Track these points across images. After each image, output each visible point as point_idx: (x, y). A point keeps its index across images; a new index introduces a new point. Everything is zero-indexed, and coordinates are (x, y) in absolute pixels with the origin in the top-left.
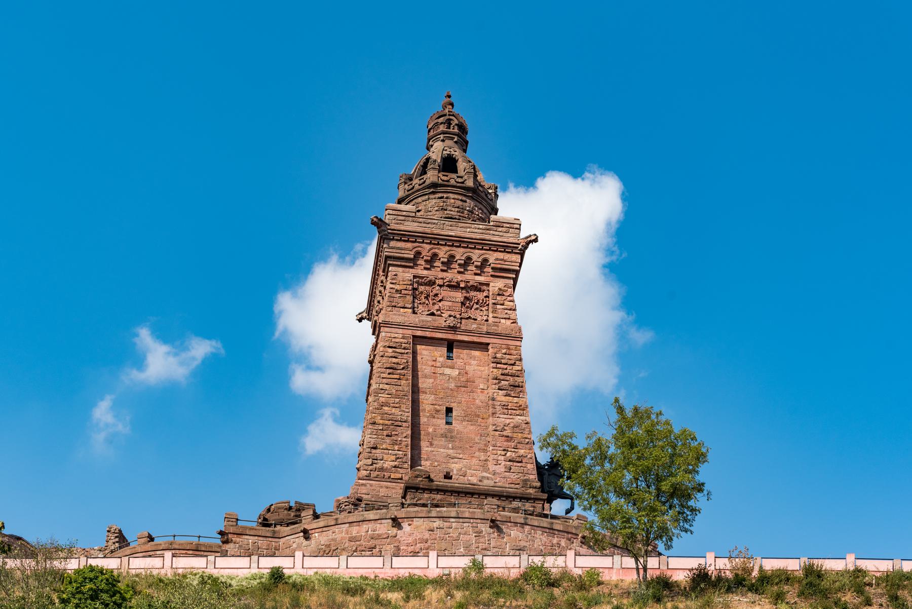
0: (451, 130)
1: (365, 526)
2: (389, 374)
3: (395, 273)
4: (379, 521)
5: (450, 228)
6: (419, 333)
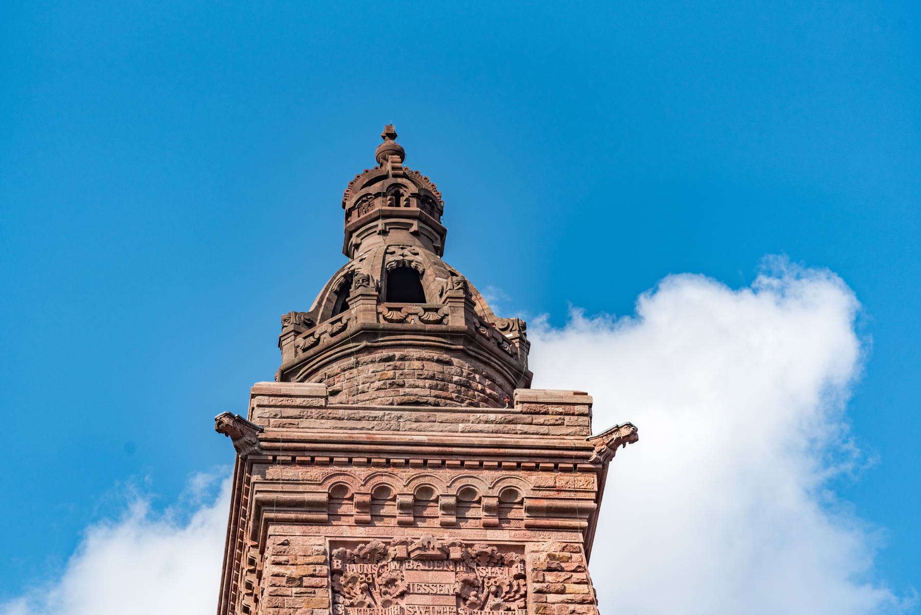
0: (402, 208)
3: (283, 539)
5: (415, 425)
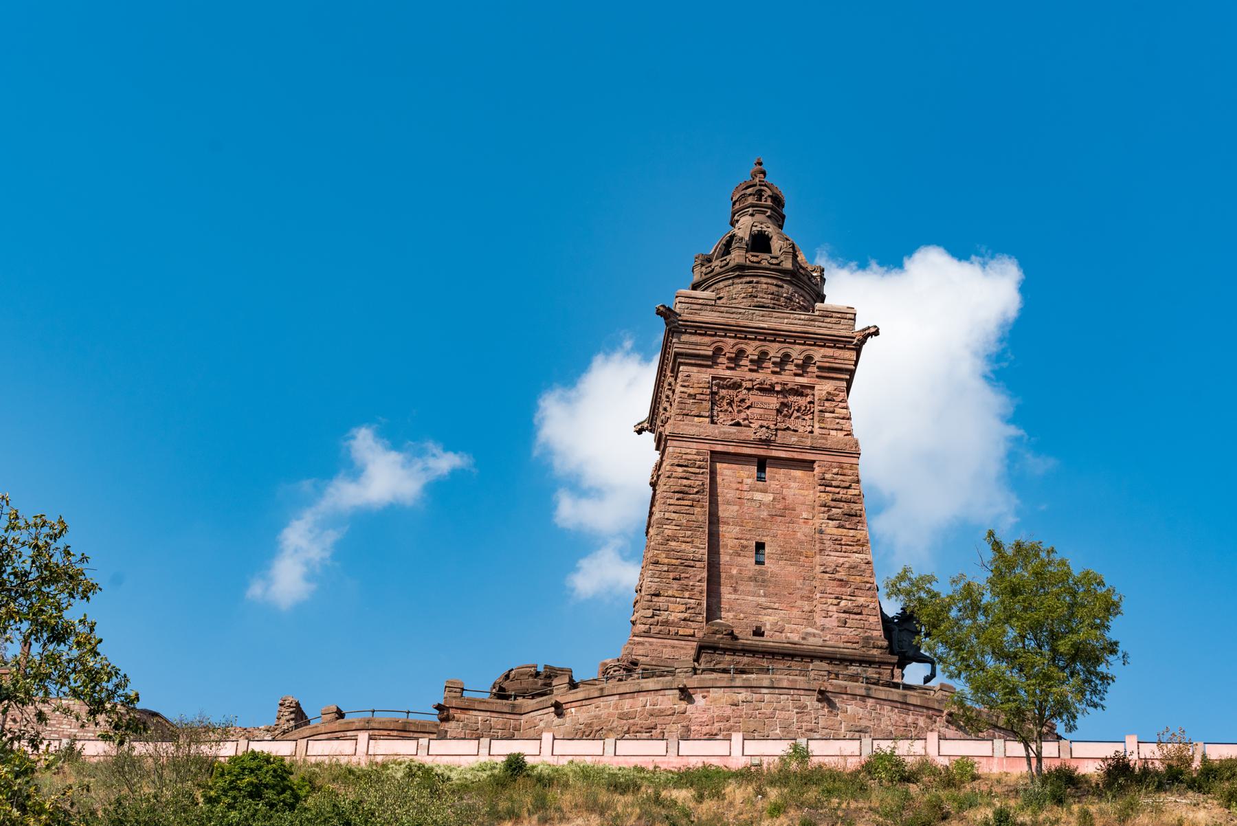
0: (763, 203)
1: (641, 699)
2: (678, 499)
4: (662, 692)
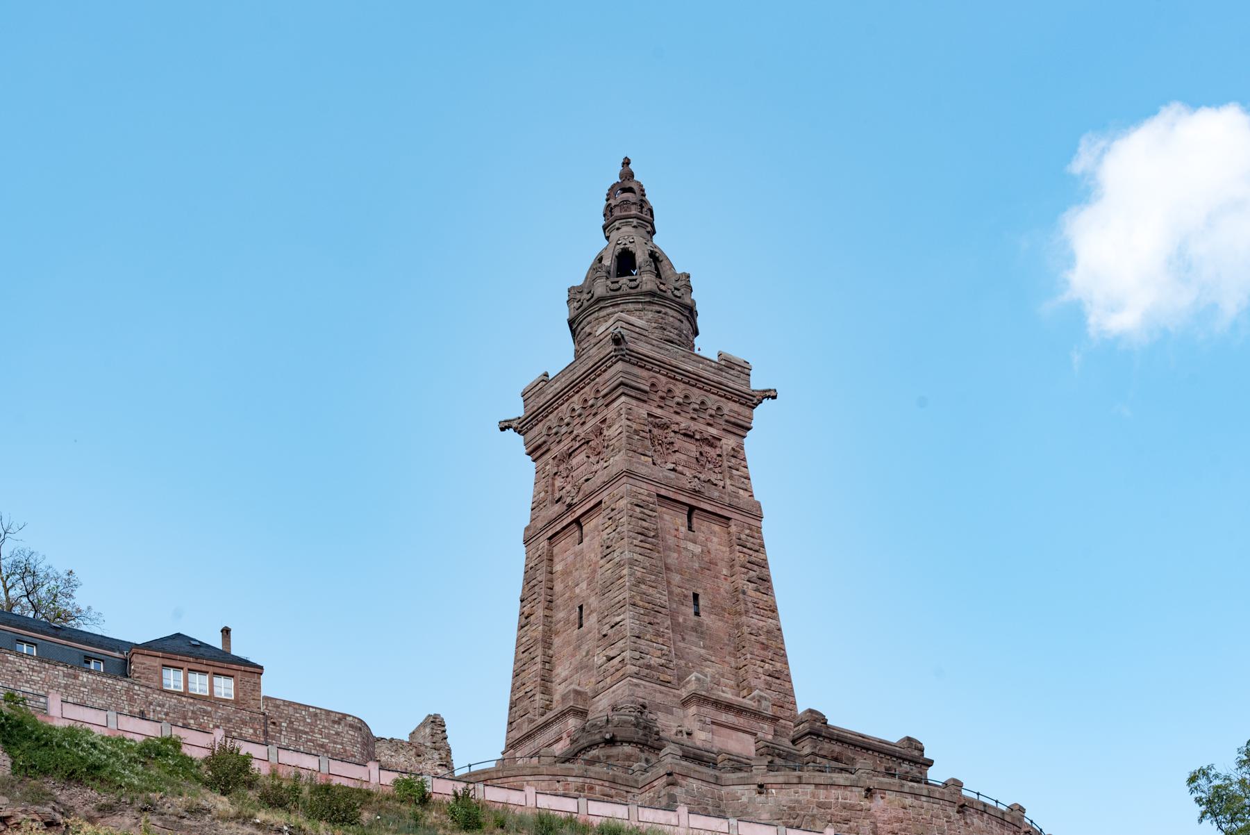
0: (644, 215)
2: (641, 541)
3: (630, 406)
5: (683, 359)
6: (663, 492)
